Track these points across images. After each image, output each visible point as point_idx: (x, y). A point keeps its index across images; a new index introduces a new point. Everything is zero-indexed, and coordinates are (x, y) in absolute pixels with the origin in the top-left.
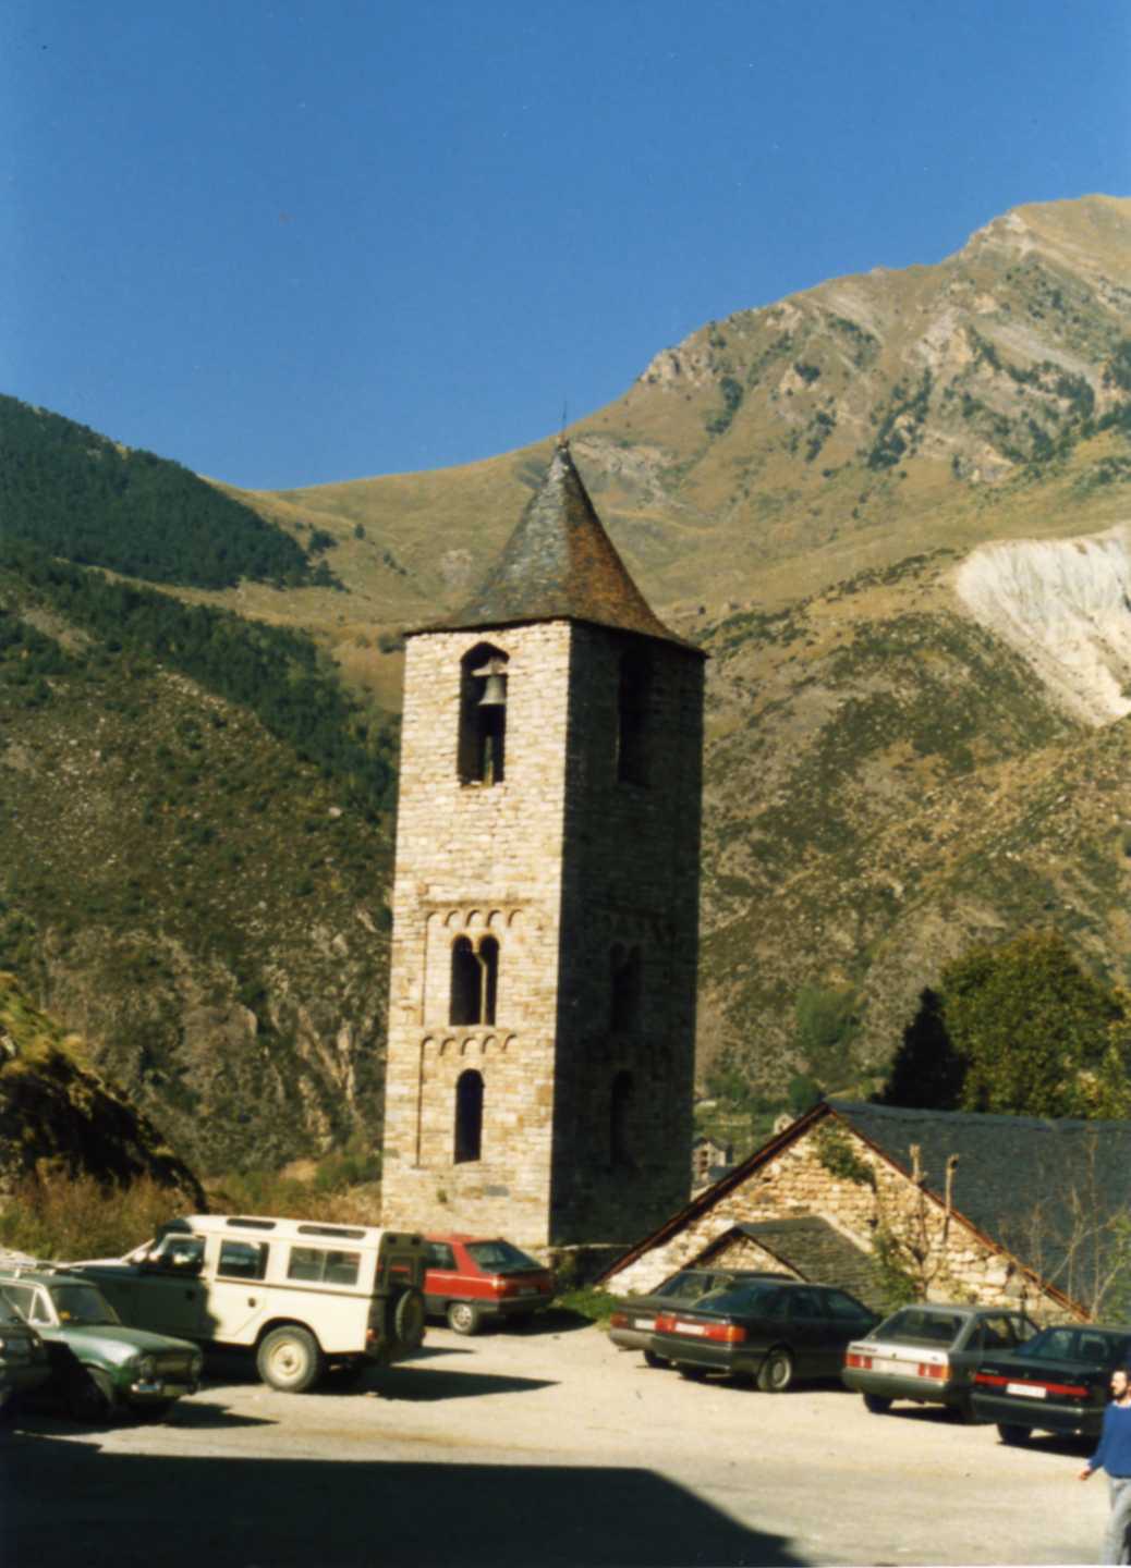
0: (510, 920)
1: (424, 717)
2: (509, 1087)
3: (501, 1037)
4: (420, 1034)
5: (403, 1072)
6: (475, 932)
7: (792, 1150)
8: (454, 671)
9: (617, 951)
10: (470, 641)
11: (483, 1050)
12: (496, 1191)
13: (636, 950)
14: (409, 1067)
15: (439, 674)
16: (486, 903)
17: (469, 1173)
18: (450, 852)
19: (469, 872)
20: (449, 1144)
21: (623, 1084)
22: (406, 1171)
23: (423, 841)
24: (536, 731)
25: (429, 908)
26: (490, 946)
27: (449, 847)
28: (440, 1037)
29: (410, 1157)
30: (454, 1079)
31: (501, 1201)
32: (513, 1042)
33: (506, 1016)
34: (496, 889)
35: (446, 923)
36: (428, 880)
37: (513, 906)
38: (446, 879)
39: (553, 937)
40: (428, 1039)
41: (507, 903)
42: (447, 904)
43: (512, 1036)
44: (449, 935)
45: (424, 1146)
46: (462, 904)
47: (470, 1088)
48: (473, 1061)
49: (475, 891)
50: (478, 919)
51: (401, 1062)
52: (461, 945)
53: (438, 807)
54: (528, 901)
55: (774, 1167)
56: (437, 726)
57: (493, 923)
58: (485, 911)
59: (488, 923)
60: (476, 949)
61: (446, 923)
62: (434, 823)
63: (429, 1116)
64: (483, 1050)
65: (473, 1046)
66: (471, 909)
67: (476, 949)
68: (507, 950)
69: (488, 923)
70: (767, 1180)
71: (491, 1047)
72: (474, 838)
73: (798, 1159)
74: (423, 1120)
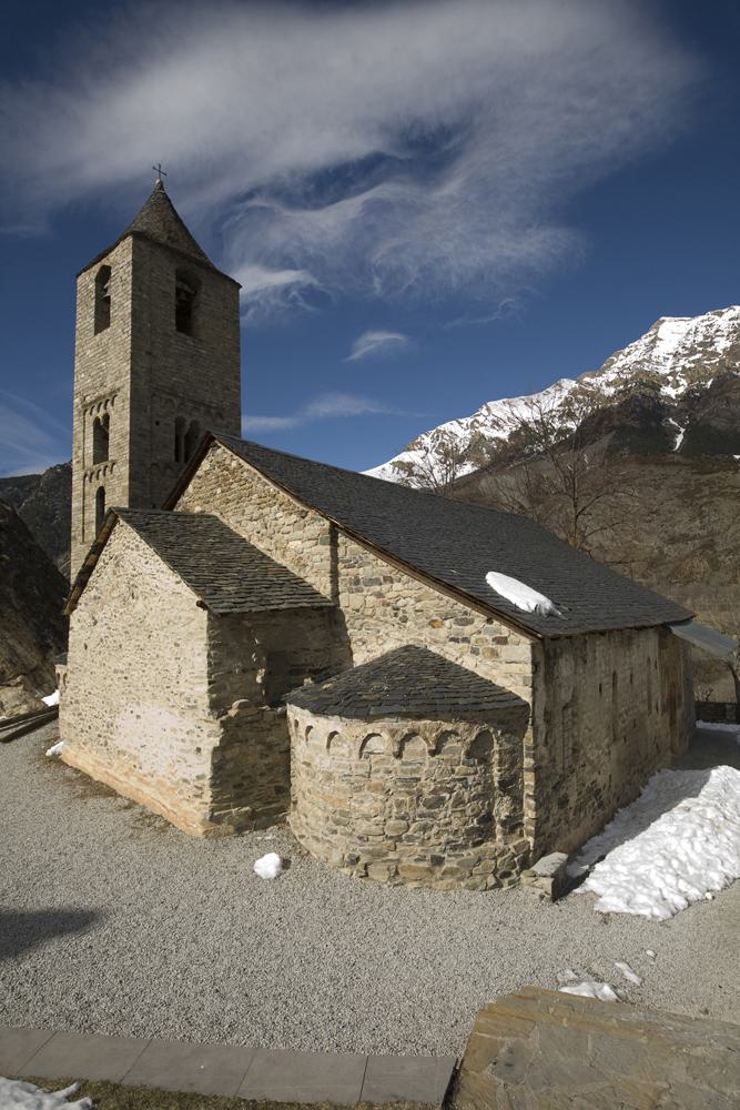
0: (112, 404)
3: (109, 464)
4: (82, 473)
6: (100, 415)
7: (199, 473)
8: (92, 286)
9: (179, 423)
10: (97, 268)
11: (104, 475)
13: (195, 424)
22: (79, 546)
25: (86, 407)
26: (107, 417)
28: (89, 473)
33: (112, 454)
34: (107, 390)
35: (91, 414)
37: (114, 393)
38: (91, 391)
39: (128, 403)
41: (111, 393)
42: (91, 403)
45: (86, 531)
47: (101, 493)
49: (101, 393)
50: (102, 407)
54: (119, 389)
55: (190, 488)
58: (103, 401)
59: (105, 408)
61: (91, 414)
64: (104, 475)
69: (105, 408)
73: (199, 477)
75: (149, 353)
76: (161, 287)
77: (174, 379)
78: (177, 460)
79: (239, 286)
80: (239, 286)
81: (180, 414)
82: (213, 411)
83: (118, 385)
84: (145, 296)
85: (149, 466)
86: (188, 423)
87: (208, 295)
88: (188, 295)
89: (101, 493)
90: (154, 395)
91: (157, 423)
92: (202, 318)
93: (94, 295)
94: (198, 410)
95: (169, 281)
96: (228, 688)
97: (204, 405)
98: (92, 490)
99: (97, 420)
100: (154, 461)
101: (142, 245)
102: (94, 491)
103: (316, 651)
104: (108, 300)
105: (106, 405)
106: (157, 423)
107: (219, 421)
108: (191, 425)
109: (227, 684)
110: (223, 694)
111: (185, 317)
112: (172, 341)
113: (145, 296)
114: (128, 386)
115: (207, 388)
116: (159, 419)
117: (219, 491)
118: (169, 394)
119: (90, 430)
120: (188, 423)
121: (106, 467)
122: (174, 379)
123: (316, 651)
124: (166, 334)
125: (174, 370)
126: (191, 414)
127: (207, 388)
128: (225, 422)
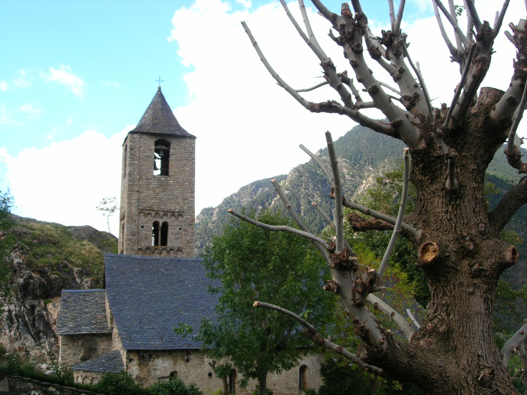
9: (156, 224)
75: (138, 191)
76: (146, 154)
77: (153, 201)
78: (156, 243)
79: (195, 138)
80: (195, 138)
81: (156, 220)
82: (176, 214)
84: (136, 162)
85: (136, 250)
86: (161, 224)
88: (164, 150)
90: (140, 212)
91: (142, 227)
94: (167, 215)
96: (68, 359)
97: (170, 212)
100: (140, 247)
103: (103, 349)
106: (142, 227)
109: (68, 358)
110: (66, 361)
112: (152, 181)
115: (172, 201)
116: (143, 225)
118: (149, 210)
120: (161, 224)
122: (153, 201)
123: (103, 349)
124: (147, 179)
127: (172, 201)
128: (184, 219)
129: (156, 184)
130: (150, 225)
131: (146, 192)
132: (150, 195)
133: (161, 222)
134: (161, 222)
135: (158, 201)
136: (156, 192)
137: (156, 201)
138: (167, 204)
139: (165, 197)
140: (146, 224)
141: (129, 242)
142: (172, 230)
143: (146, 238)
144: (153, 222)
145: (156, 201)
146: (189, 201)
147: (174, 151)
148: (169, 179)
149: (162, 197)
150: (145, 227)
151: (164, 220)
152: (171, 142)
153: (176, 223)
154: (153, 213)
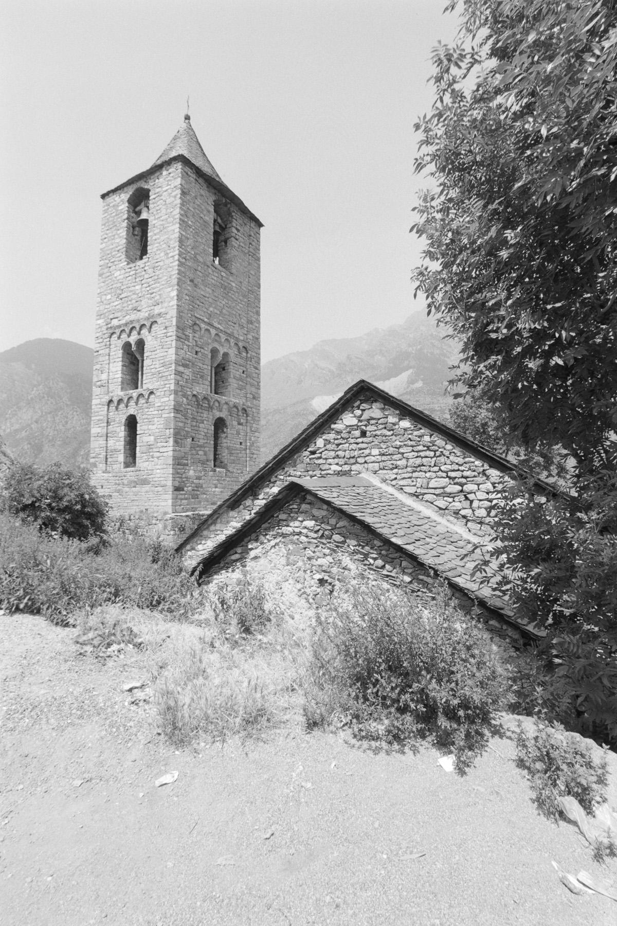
1: (110, 235)
2: (150, 422)
3: (146, 394)
4: (106, 399)
5: (99, 420)
6: (133, 339)
8: (124, 207)
9: (214, 352)
10: (130, 191)
12: (145, 482)
13: (226, 355)
14: (102, 418)
15: (117, 210)
16: (138, 321)
17: (130, 473)
18: (121, 299)
19: (130, 307)
20: (121, 458)
21: (220, 425)
23: (109, 297)
24: (164, 222)
26: (141, 344)
27: (121, 297)
29: (102, 466)
30: (123, 421)
31: (147, 488)
32: (152, 396)
33: (148, 381)
34: (143, 315)
35: (119, 338)
36: (111, 316)
40: (111, 401)
42: (119, 326)
43: (152, 393)
44: (120, 343)
45: (109, 460)
46: (126, 324)
48: (132, 411)
49: (133, 316)
50: (134, 333)
51: (99, 415)
52: (127, 346)
53: (116, 277)
54: (159, 314)
55: (320, 442)
56: (116, 236)
57: (142, 332)
59: (139, 334)
60: (134, 348)
61: (119, 338)
62: (114, 286)
63: (111, 442)
64: (137, 403)
65: (132, 403)
66: (131, 326)
67: (134, 348)
68: (150, 343)
69: (139, 334)
70: (313, 453)
71: (142, 401)
72: (133, 288)
73: (339, 432)
74: (109, 445)
75: (192, 281)
80: (260, 225)
81: (216, 345)
83: (157, 310)
87: (238, 230)
89: (132, 423)
91: (197, 352)
92: (233, 251)
93: (126, 216)
95: (209, 211)
98: (121, 417)
99: (127, 345)
101: (187, 169)
102: (123, 419)
104: (145, 223)
105: (141, 329)
107: (244, 354)
108: (223, 355)
111: (219, 244)
112: (210, 271)
113: (190, 223)
114: (173, 313)
115: (235, 320)
116: (198, 349)
117: (375, 452)
119: (118, 353)
121: (131, 397)
122: (211, 309)
125: (210, 300)
126: (222, 346)
129: (215, 278)
130: (206, 352)
131: (202, 287)
132: (207, 295)
133: (222, 351)
134: (222, 351)
135: (218, 312)
136: (215, 294)
137: (216, 311)
138: (230, 323)
139: (226, 308)
140: (202, 350)
141: (179, 378)
142: (234, 371)
143: (202, 377)
144: (210, 347)
145: (216, 311)
146: (254, 327)
147: (236, 232)
148: (231, 278)
149: (222, 305)
150: (200, 354)
151: (226, 350)
152: (233, 214)
153: (239, 361)
154: (213, 332)
